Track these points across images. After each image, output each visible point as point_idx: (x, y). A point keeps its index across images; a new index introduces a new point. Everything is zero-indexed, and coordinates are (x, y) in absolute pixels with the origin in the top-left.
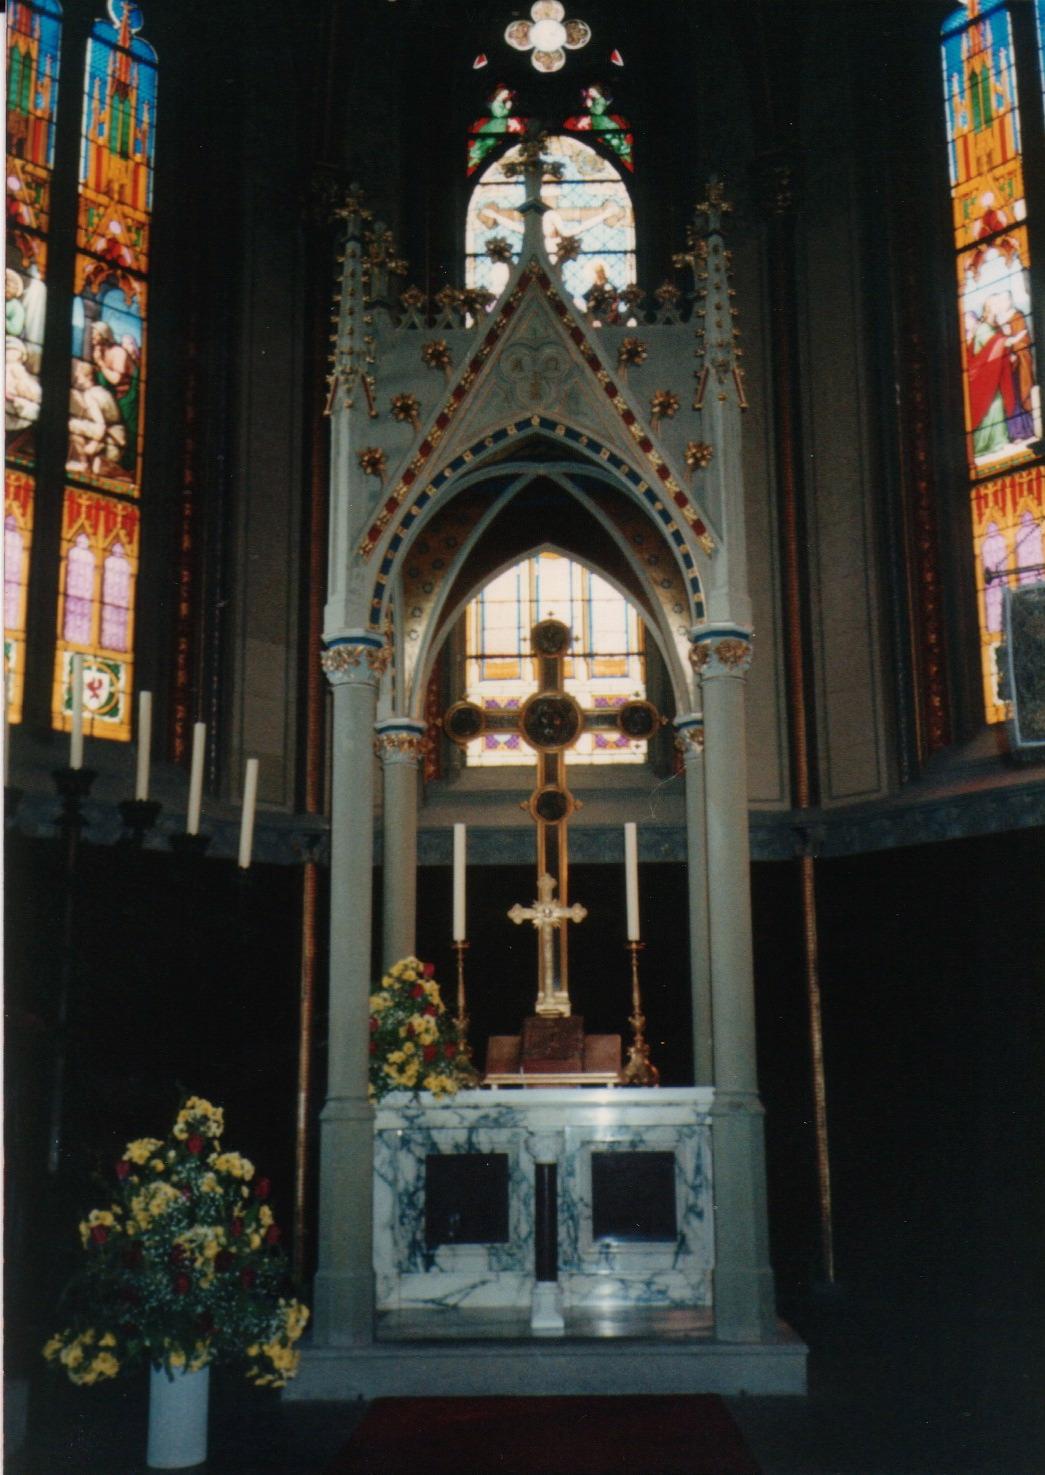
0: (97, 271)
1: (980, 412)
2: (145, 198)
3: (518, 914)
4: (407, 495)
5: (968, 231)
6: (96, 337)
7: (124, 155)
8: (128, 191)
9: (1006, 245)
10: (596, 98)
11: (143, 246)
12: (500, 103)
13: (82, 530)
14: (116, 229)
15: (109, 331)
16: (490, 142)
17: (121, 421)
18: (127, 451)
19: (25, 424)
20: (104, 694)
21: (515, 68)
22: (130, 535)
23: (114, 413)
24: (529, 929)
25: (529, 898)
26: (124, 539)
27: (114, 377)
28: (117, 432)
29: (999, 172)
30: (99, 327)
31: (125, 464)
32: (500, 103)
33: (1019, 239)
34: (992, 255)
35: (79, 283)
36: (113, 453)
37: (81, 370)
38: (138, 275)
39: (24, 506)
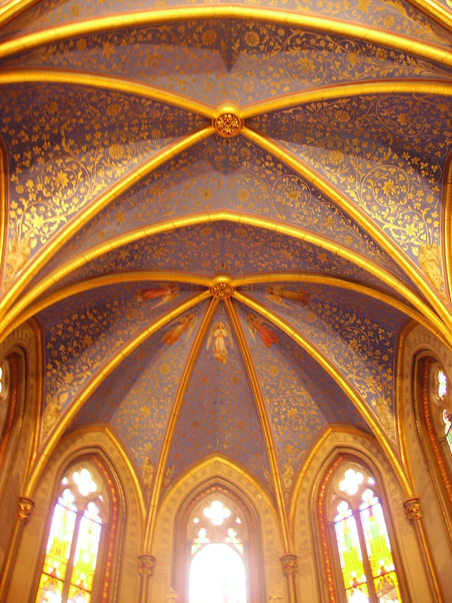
5: (348, 583)
9: (360, 589)
12: (202, 532)
33: (365, 587)
38: (88, 591)
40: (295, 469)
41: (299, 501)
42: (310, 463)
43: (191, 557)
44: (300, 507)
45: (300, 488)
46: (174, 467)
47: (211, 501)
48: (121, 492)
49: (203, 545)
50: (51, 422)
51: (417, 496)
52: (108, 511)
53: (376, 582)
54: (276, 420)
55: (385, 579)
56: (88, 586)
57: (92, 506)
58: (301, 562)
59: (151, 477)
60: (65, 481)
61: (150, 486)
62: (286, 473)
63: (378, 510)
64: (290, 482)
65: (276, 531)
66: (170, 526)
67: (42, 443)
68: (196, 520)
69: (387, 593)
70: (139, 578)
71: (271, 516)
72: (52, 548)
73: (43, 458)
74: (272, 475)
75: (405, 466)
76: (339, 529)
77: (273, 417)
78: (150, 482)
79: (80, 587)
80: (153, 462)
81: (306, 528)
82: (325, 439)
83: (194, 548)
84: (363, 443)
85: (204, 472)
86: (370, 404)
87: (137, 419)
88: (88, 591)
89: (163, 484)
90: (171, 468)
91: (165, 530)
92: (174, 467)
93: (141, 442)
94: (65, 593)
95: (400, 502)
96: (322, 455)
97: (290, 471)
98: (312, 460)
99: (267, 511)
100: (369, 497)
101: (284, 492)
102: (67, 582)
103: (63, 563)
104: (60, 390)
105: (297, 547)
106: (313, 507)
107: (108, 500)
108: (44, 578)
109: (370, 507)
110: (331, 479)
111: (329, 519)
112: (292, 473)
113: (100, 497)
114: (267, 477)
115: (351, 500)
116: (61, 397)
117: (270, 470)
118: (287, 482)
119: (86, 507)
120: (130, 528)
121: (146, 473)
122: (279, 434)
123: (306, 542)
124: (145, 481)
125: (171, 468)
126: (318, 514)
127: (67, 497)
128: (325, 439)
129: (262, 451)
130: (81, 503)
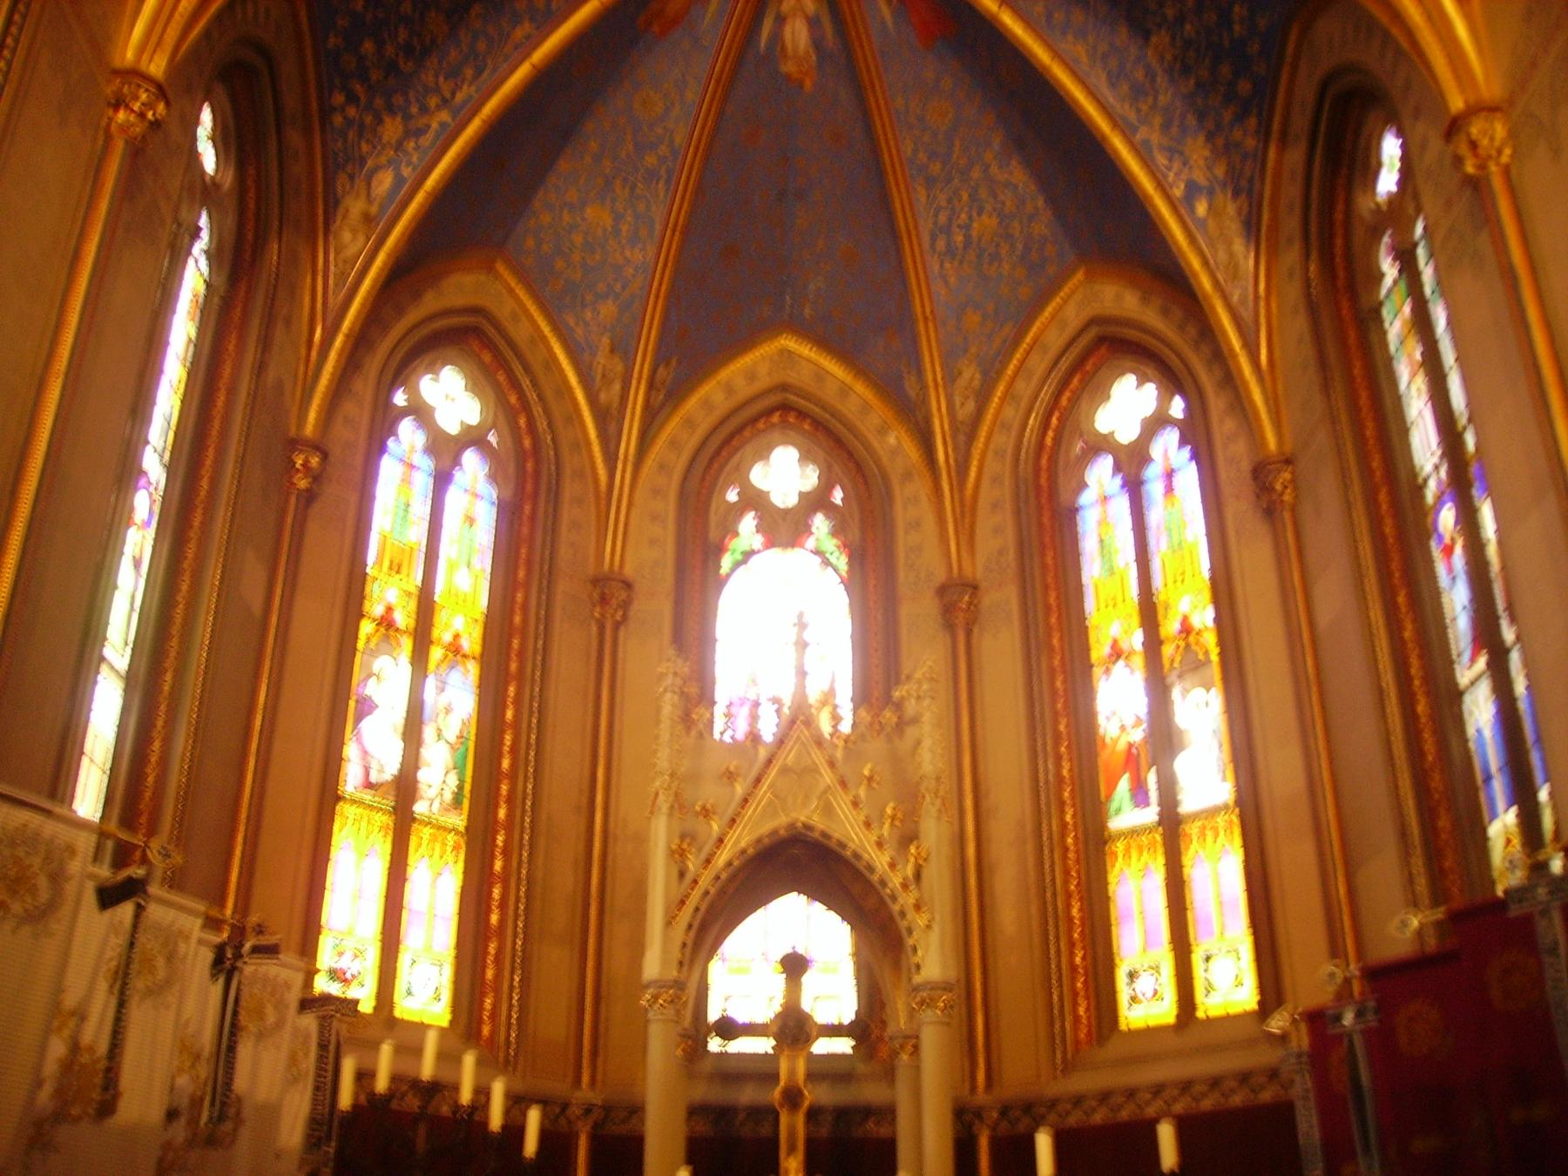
1: (1112, 786)
4: (705, 881)
5: (1099, 650)
12: (748, 523)
32: (748, 523)
33: (1138, 661)
34: (1119, 667)
35: (432, 665)
36: (448, 796)
37: (429, 733)
40: (985, 373)
41: (990, 454)
42: (1023, 362)
43: (721, 582)
44: (992, 466)
45: (994, 423)
46: (674, 362)
47: (770, 449)
48: (542, 424)
49: (748, 555)
51: (1288, 448)
52: (511, 469)
53: (1168, 650)
54: (941, 244)
55: (1188, 646)
56: (472, 641)
57: (471, 458)
58: (988, 600)
59: (617, 387)
60: (400, 399)
61: (615, 412)
62: (962, 382)
63: (1189, 478)
64: (971, 406)
65: (930, 521)
66: (669, 507)
67: (335, 301)
68: (732, 496)
70: (594, 629)
71: (920, 487)
72: (379, 561)
73: (339, 341)
74: (924, 387)
75: (1267, 377)
76: (1089, 523)
77: (933, 238)
78: (616, 400)
79: (455, 649)
80: (623, 349)
81: (1006, 518)
82: (1065, 301)
83: (726, 562)
84: (1165, 312)
85: (751, 376)
86: (1192, 210)
87: (578, 239)
89: (647, 405)
90: (668, 364)
91: (655, 517)
92: (674, 362)
93: (589, 298)
94: (420, 658)
95: (1246, 466)
96: (1055, 340)
97: (972, 379)
98: (1028, 353)
99: (907, 476)
100: (1168, 448)
101: (955, 427)
103: (409, 594)
104: (370, 163)
105: (981, 560)
106: (1026, 468)
107: (510, 443)
108: (366, 627)
110: (1075, 401)
111: (1064, 496)
112: (976, 383)
113: (492, 438)
114: (912, 393)
115: (1123, 457)
116: (374, 184)
117: (920, 372)
119: (456, 462)
120: (567, 513)
122: (946, 282)
123: (1001, 552)
124: (603, 397)
125: (668, 364)
126: (1038, 488)
127: (409, 436)
128: (1065, 301)
129: (902, 324)
130: (445, 453)
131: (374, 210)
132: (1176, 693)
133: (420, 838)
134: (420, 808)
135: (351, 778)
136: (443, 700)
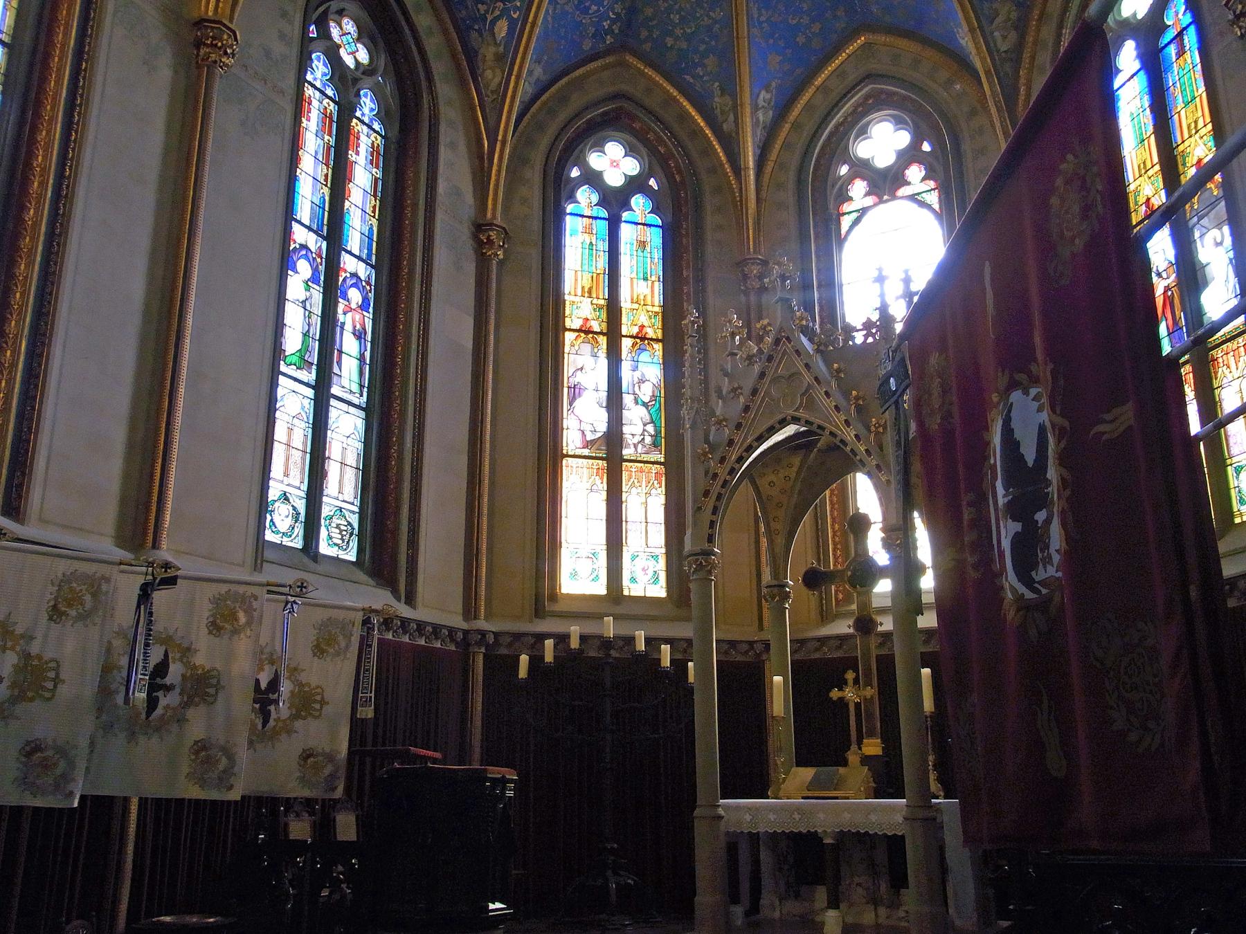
0: (634, 345)
2: (658, 299)
3: (835, 694)
6: (636, 380)
7: (645, 279)
8: (649, 298)
10: (915, 173)
11: (659, 324)
12: (858, 189)
13: (633, 485)
14: (643, 319)
15: (643, 375)
16: (855, 215)
17: (652, 422)
18: (655, 437)
19: (599, 435)
20: (650, 573)
21: (863, 169)
22: (660, 483)
23: (647, 418)
24: (842, 702)
25: (841, 684)
26: (657, 485)
27: (647, 399)
28: (650, 428)
29: (1150, 173)
30: (637, 374)
31: (655, 445)
32: (858, 189)
36: (648, 440)
37: (628, 400)
38: (657, 340)
39: (602, 479)
43: (841, 241)
49: (863, 211)
50: (497, 80)
57: (639, 203)
59: (732, 117)
67: (492, 123)
68: (575, 173)
69: (1206, 215)
78: (733, 126)
79: (641, 338)
83: (846, 222)
87: (676, 19)
88: (657, 340)
97: (1009, 12)
102: (613, 333)
103: (600, 307)
104: (489, 18)
108: (569, 337)
109: (1180, 35)
113: (652, 182)
116: (496, 30)
118: (1004, 37)
121: (723, 112)
124: (725, 126)
127: (585, 197)
130: (614, 202)
131: (501, 49)
132: (1197, 234)
133: (629, 473)
134: (627, 452)
135: (571, 440)
136: (637, 374)
